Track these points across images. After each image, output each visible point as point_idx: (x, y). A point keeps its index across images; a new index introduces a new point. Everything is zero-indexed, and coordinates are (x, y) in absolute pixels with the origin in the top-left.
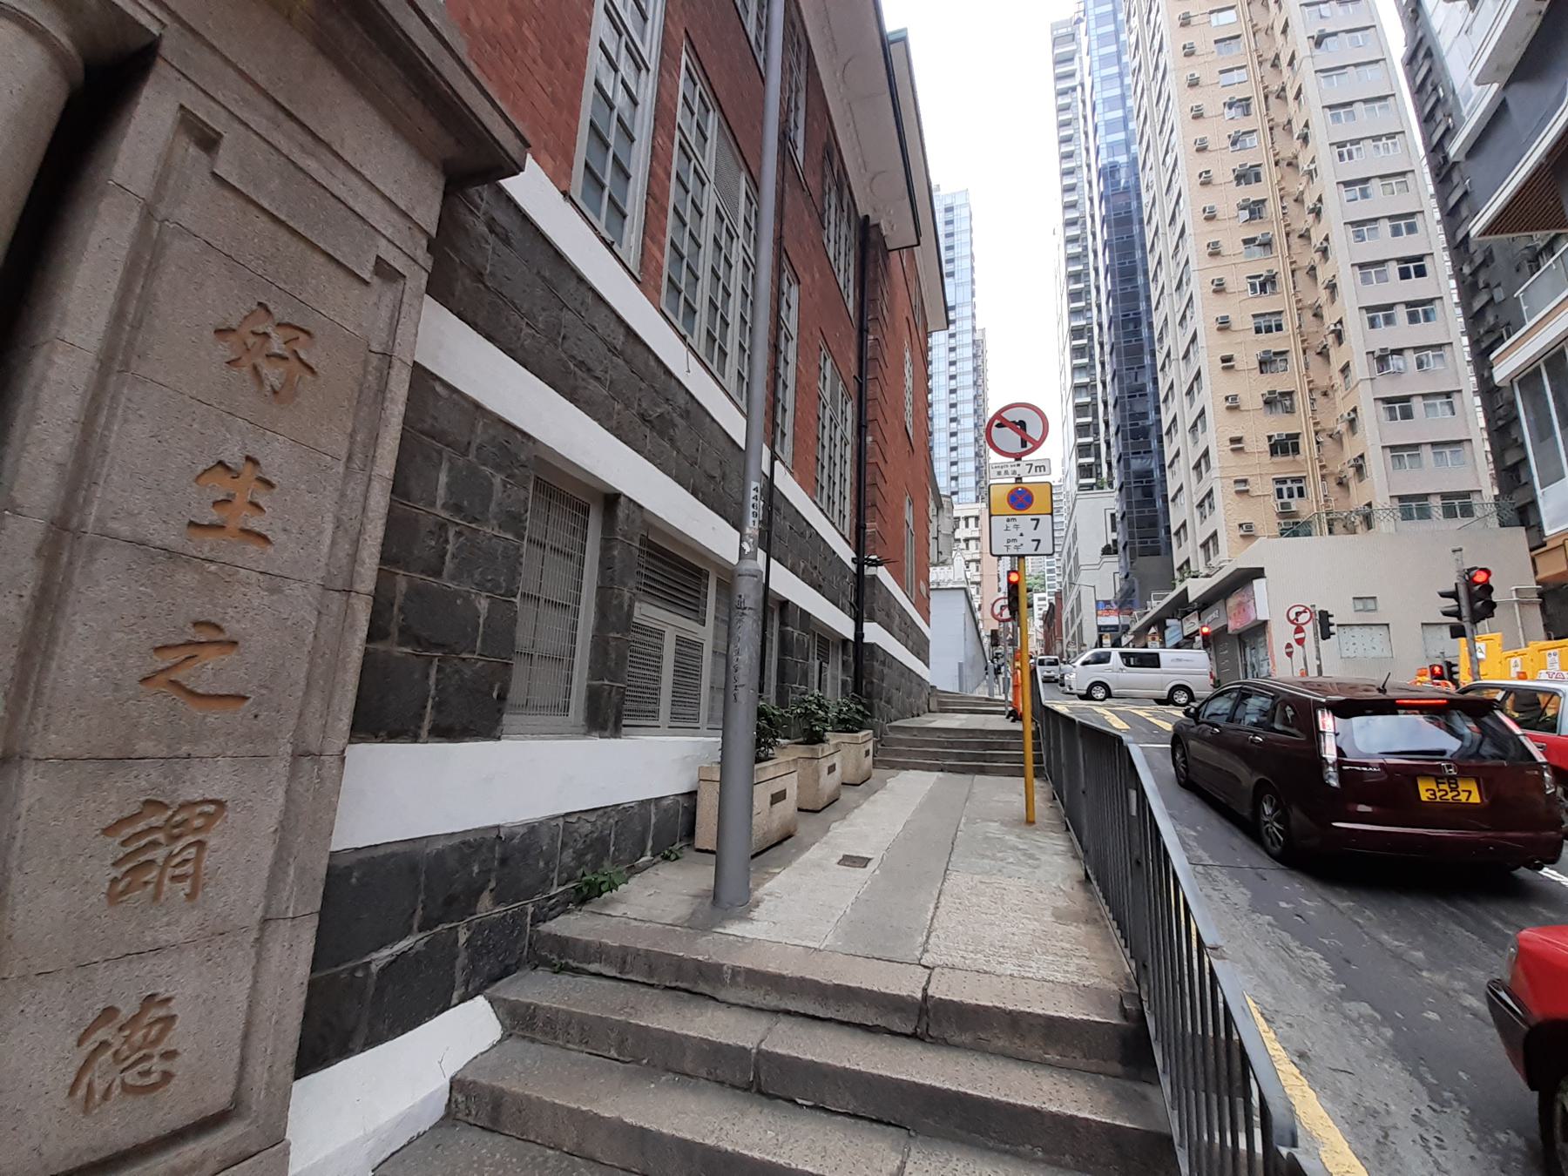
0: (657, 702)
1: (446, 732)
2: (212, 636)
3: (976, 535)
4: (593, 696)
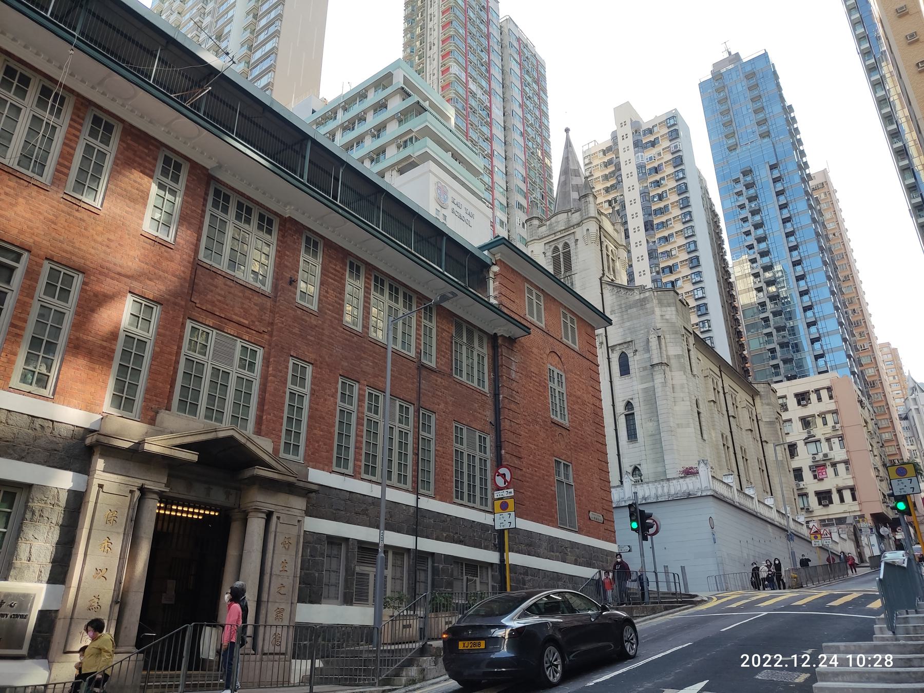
0: (367, 596)
1: (312, 602)
2: (283, 586)
3: (832, 407)
4: (345, 594)
